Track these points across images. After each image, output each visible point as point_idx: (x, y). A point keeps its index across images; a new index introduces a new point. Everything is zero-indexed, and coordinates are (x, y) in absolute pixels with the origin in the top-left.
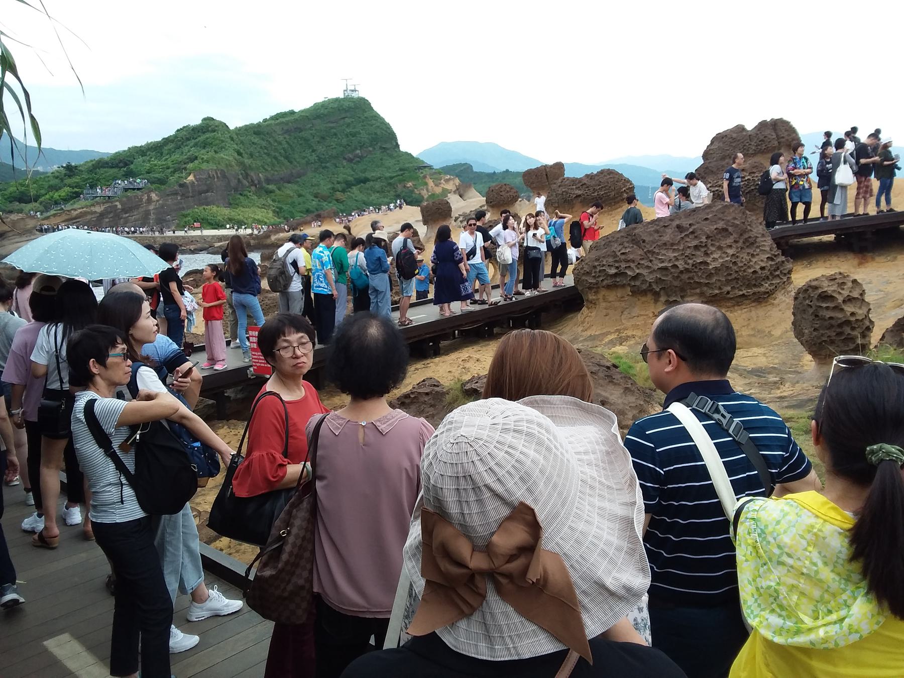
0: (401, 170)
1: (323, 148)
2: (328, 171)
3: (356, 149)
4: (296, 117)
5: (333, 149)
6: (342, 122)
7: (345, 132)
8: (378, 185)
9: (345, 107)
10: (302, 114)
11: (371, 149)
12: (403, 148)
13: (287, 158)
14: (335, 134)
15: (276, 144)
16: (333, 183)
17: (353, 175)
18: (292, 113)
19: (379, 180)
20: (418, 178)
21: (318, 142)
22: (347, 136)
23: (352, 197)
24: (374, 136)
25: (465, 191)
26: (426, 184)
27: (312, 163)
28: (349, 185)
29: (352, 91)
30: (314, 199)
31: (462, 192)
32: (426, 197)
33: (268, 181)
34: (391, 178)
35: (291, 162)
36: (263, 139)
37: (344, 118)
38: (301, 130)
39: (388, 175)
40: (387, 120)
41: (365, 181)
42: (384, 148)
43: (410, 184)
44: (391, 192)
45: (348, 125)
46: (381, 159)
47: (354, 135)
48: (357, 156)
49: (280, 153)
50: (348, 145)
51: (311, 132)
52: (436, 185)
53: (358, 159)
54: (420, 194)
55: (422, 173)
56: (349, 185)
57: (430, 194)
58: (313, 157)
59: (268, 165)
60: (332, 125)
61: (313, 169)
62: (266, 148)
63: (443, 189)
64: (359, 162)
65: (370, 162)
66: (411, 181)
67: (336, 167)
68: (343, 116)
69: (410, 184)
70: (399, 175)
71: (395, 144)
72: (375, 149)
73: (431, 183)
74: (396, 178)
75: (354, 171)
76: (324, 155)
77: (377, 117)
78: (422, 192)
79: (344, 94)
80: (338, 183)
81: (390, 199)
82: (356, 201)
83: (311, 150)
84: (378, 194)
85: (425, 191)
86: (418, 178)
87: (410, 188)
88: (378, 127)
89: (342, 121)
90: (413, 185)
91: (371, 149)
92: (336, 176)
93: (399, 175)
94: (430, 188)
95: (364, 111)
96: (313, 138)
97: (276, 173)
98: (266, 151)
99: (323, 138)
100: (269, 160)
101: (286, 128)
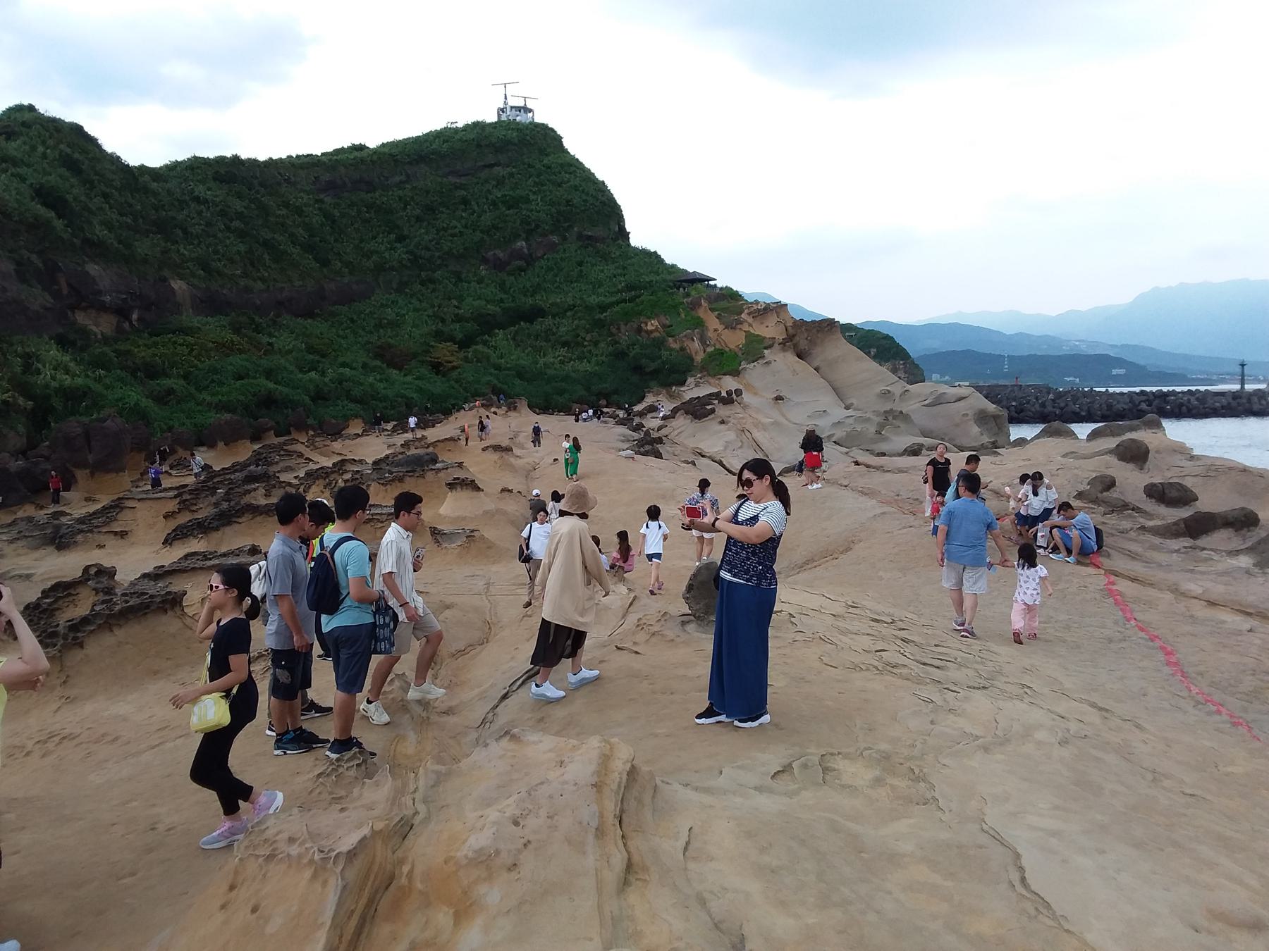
0: (630, 288)
1: (427, 233)
2: (434, 290)
3: (517, 237)
4: (364, 154)
5: (453, 235)
6: (484, 174)
7: (490, 197)
8: (565, 327)
9: (494, 140)
10: (386, 150)
11: (555, 239)
12: (638, 239)
13: (309, 248)
14: (465, 202)
15: (284, 212)
16: (443, 321)
17: (502, 301)
18: (361, 148)
19: (569, 314)
20: (675, 307)
21: (418, 219)
22: (494, 204)
23: (488, 358)
24: (563, 208)
25: (813, 343)
26: (700, 324)
27: (392, 268)
28: (487, 324)
29: (518, 109)
30: (320, 359)
31: (803, 344)
32: (699, 357)
33: (211, 304)
34: (603, 308)
35: (325, 263)
36: (239, 196)
37: (491, 166)
38: (371, 187)
39: (594, 300)
40: (600, 176)
41: (535, 314)
42: (589, 238)
43: (655, 322)
44: (602, 345)
45: (500, 183)
46: (580, 264)
47: (513, 204)
48: (518, 255)
49: (292, 235)
50: (497, 228)
51: (400, 192)
52: (730, 326)
53: (522, 263)
54: (682, 349)
55: (688, 295)
56: (487, 324)
57: (710, 349)
58: (400, 253)
59: (232, 261)
60: (452, 179)
61: (394, 286)
62: (240, 216)
63: (748, 334)
64: (521, 269)
65: (550, 269)
66: (657, 316)
67: (460, 280)
68: (490, 159)
69: (652, 325)
70: (624, 301)
71: (617, 229)
72: (565, 239)
73: (713, 322)
74: (616, 309)
75: (505, 293)
76: (428, 249)
77: (575, 167)
78: (687, 343)
79: (499, 116)
80: (458, 319)
81: (597, 364)
82: (498, 368)
83: (392, 236)
84: (563, 351)
85: (696, 344)
86: (675, 307)
87: (656, 334)
88: (576, 188)
89: (487, 171)
90: (664, 326)
91: (555, 239)
92: (455, 302)
93: (624, 301)
94: (710, 334)
95: (543, 152)
96: (405, 208)
97: (260, 285)
98: (236, 224)
99: (430, 209)
100: (242, 248)
101: (326, 177)
